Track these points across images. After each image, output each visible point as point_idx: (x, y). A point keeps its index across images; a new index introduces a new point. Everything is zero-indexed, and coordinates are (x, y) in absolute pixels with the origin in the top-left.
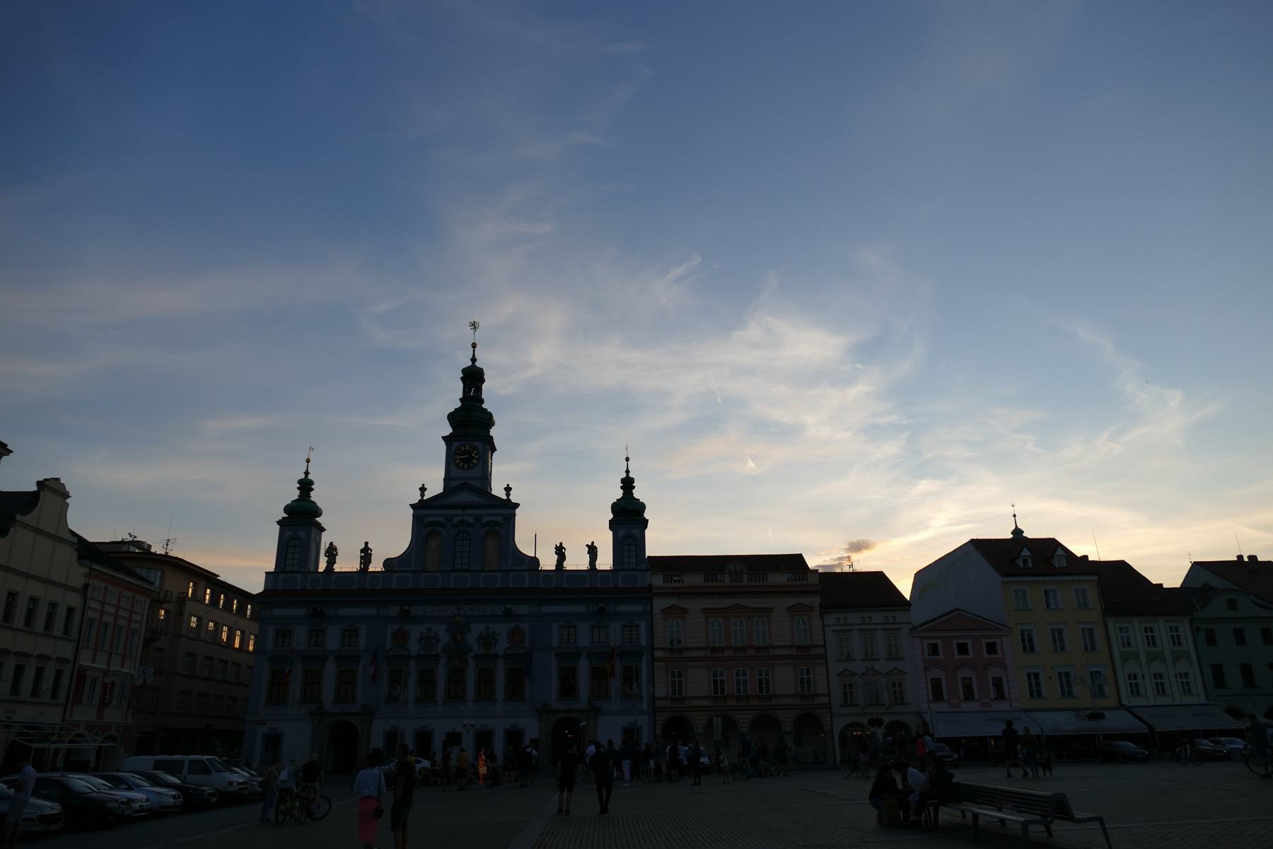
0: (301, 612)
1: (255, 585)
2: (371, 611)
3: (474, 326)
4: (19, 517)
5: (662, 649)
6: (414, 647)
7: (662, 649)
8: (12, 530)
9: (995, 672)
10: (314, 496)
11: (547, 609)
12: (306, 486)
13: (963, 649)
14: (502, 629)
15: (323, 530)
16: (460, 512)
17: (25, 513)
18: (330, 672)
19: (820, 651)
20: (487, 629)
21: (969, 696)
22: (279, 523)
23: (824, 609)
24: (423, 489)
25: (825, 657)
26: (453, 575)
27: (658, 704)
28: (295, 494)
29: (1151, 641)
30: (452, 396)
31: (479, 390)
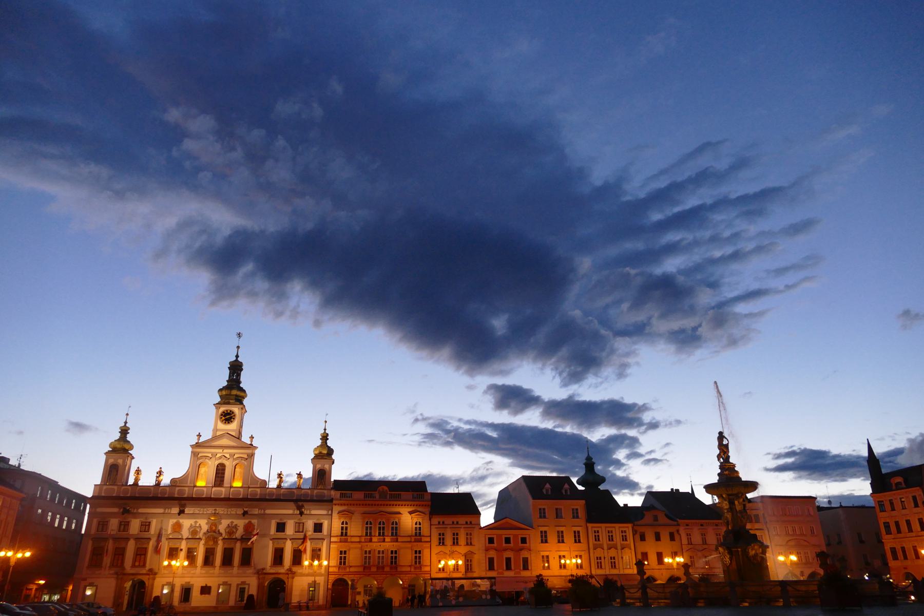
0: (115, 510)
1: (89, 493)
2: (161, 511)
3: (239, 335)
6: (185, 533)
10: (129, 437)
11: (268, 512)
12: (124, 431)
13: (508, 540)
14: (241, 523)
15: (133, 458)
18: (131, 547)
22: (106, 453)
24: (199, 435)
28: (117, 436)
29: (611, 539)
30: (223, 379)
31: (239, 375)
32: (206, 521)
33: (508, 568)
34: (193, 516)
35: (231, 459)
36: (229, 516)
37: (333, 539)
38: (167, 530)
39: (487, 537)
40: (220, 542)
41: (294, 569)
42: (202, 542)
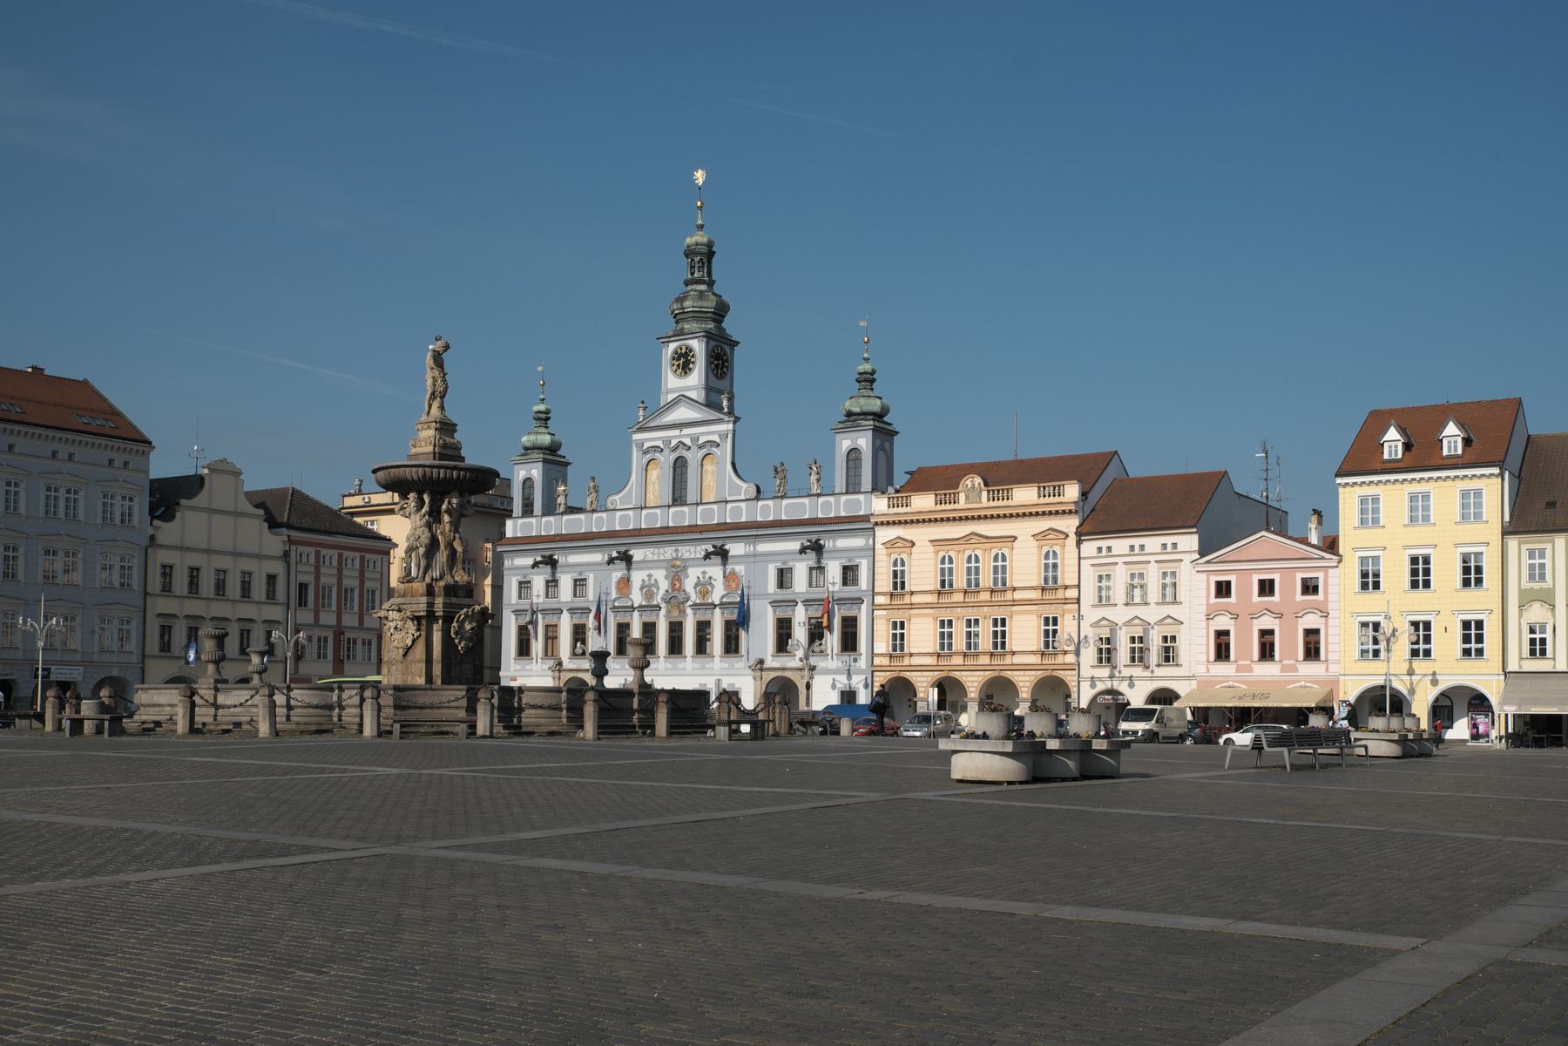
2: (597, 557)
4: (183, 502)
5: (883, 594)
6: (637, 598)
7: (883, 594)
8: (178, 515)
9: (1311, 621)
11: (764, 547)
13: (1266, 587)
14: (715, 571)
15: (567, 464)
16: (677, 432)
17: (191, 496)
19: (1072, 593)
20: (704, 573)
21: (1267, 652)
23: (1081, 535)
25: (1078, 601)
26: (672, 510)
27: (877, 661)
32: (664, 572)
33: (1267, 652)
34: (645, 564)
35: (694, 448)
36: (694, 562)
37: (880, 600)
38: (607, 594)
39: (1214, 579)
40: (689, 611)
41: (813, 661)
42: (663, 612)
